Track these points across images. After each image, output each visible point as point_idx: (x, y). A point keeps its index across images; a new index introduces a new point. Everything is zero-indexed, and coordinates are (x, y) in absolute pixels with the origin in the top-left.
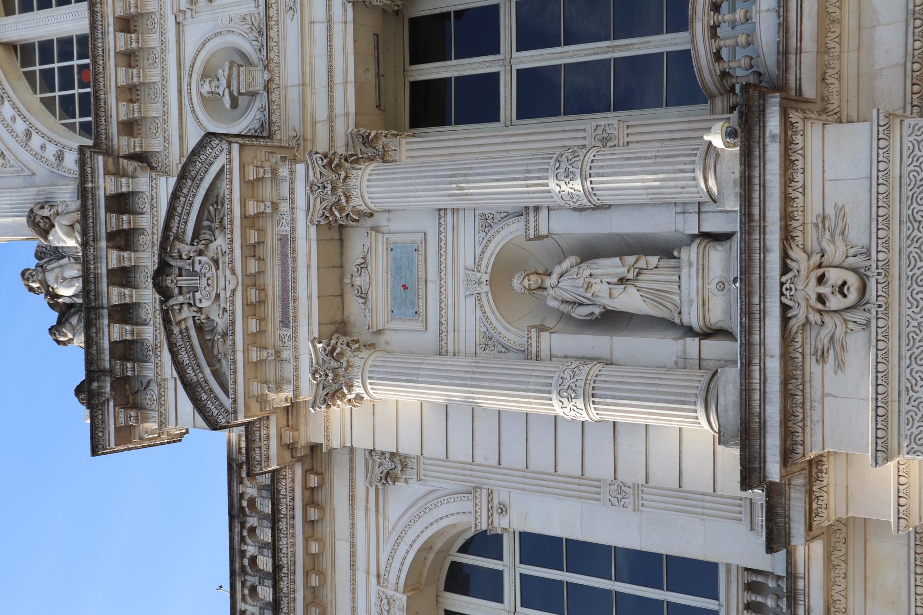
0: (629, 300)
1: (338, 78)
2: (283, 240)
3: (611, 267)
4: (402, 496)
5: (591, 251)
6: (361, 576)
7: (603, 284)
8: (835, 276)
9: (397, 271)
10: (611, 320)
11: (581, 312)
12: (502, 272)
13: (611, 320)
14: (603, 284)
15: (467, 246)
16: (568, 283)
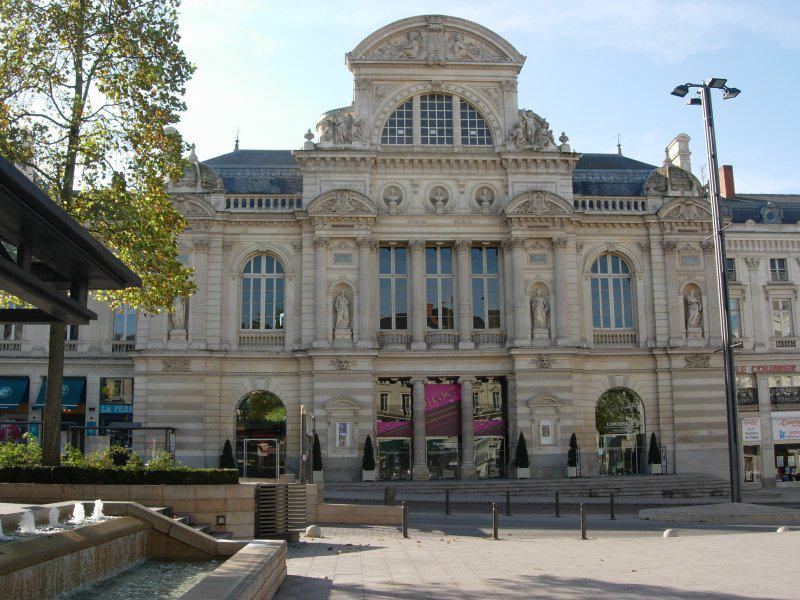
0: (340, 317)
1: (392, 236)
2: (353, 226)
3: (347, 315)
4: (289, 248)
5: (350, 306)
6: (269, 237)
7: (343, 311)
8: (345, 365)
9: (344, 256)
10: (335, 312)
11: (337, 305)
12: (344, 285)
13: (335, 312)
14: (343, 311)
15: (350, 277)
16: (343, 303)
